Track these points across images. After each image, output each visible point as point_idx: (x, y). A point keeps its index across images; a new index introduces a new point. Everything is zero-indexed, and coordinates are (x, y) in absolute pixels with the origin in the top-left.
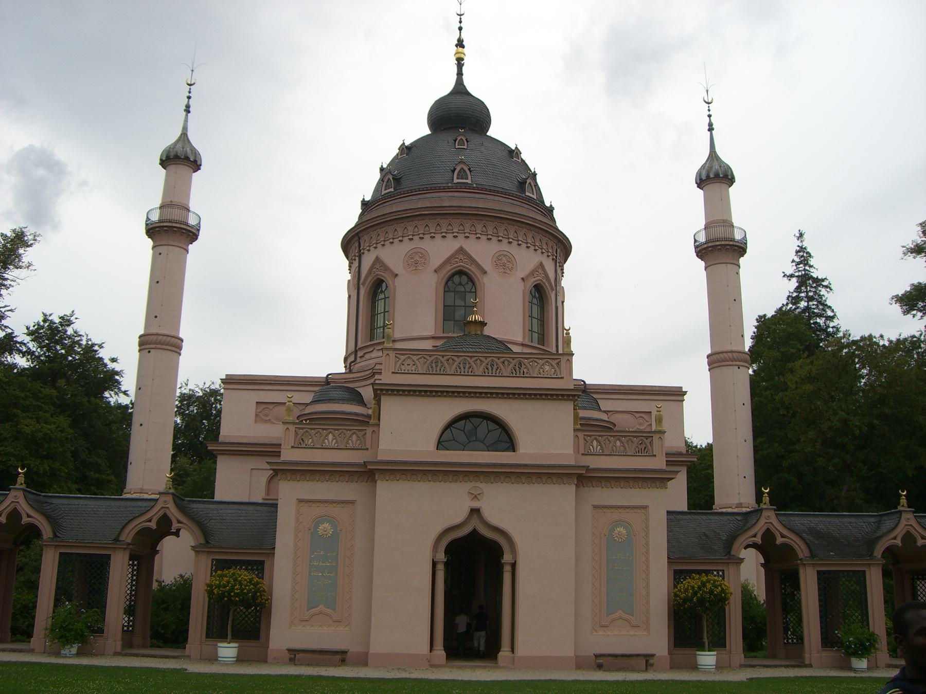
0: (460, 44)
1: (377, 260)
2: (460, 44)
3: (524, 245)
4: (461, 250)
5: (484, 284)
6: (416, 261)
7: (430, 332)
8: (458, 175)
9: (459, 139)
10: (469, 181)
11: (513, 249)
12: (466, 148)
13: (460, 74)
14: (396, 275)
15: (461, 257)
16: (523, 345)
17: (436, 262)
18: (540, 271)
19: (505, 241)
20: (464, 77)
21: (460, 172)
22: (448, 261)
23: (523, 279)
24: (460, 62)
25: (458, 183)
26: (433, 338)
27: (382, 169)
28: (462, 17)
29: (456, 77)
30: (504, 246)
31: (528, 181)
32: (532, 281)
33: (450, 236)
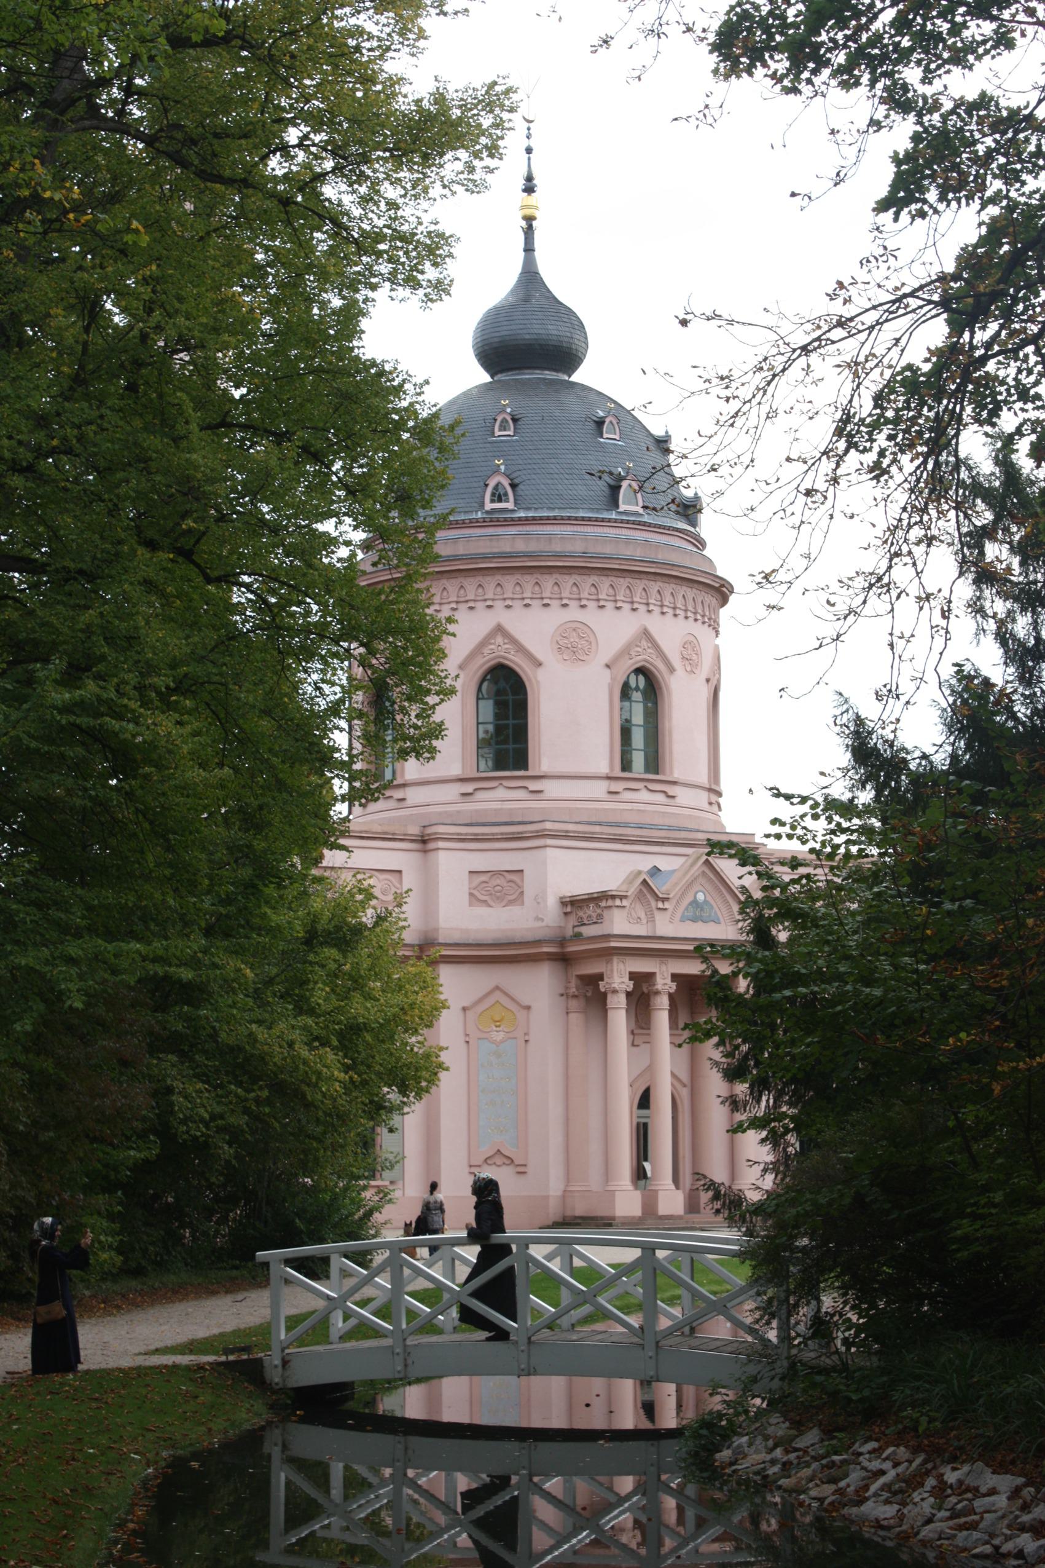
0: (529, 189)
2: (529, 189)
3: (610, 605)
4: (499, 629)
5: (538, 682)
8: (493, 495)
9: (499, 419)
11: (591, 617)
12: (511, 433)
13: (529, 249)
15: (499, 640)
16: (609, 778)
18: (644, 643)
19: (573, 604)
20: (537, 254)
21: (496, 487)
24: (529, 232)
25: (493, 511)
28: (531, 125)
29: (521, 255)
30: (573, 613)
31: (625, 484)
33: (480, 605)
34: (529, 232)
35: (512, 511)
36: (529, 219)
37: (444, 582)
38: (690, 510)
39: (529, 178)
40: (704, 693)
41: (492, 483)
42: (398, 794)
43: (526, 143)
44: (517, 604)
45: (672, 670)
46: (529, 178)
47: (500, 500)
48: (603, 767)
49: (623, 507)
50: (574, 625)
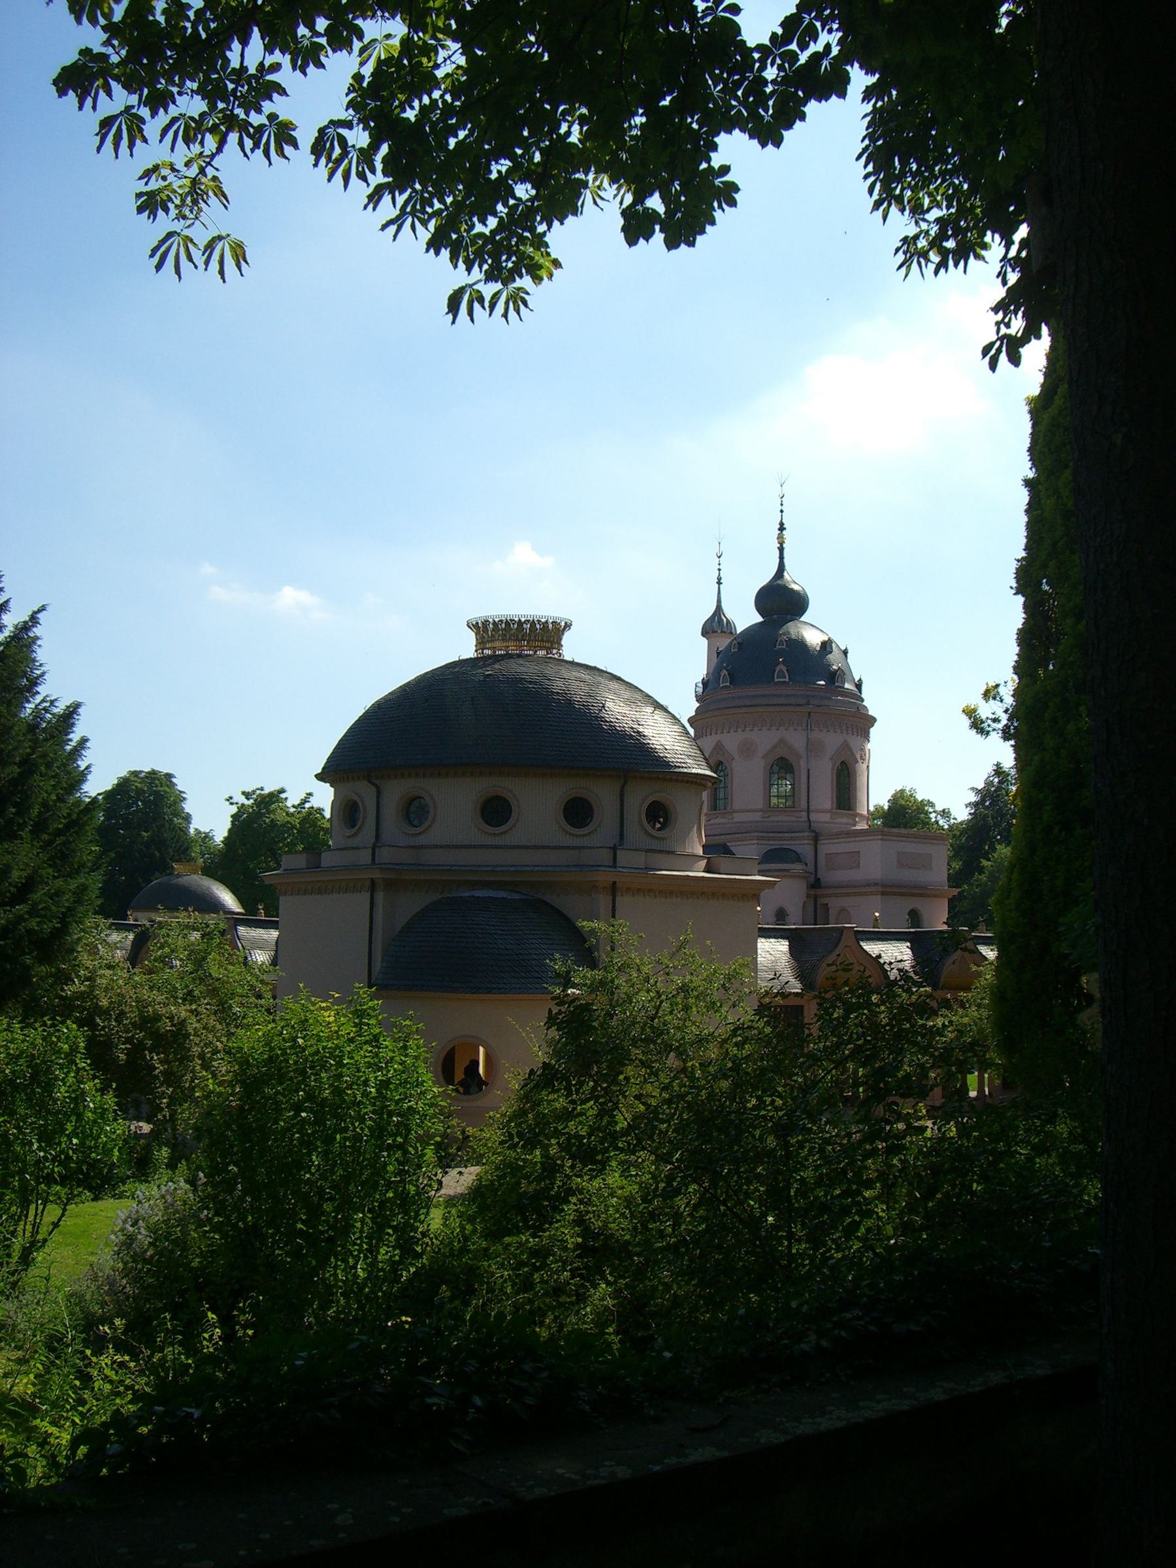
0: (782, 528)
1: (719, 747)
2: (782, 528)
6: (747, 750)
10: (787, 680)
13: (781, 557)
16: (830, 811)
24: (781, 549)
29: (778, 560)
34: (781, 549)
39: (782, 524)
41: (777, 669)
43: (780, 508)
46: (782, 524)
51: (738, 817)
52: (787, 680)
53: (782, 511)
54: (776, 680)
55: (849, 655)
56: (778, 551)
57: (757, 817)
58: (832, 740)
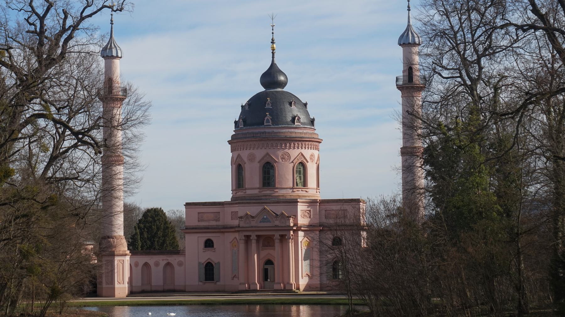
0: (273, 42)
1: (239, 156)
2: (273, 42)
7: (258, 186)
10: (270, 124)
13: (273, 57)
14: (245, 163)
15: (268, 156)
17: (258, 158)
21: (267, 120)
22: (263, 158)
23: (292, 162)
24: (273, 53)
26: (259, 188)
27: (242, 106)
32: (297, 162)
34: (273, 53)
35: (271, 125)
36: (273, 50)
37: (255, 143)
38: (312, 122)
40: (315, 166)
41: (266, 118)
42: (244, 191)
44: (272, 148)
45: (308, 162)
47: (268, 123)
48: (291, 186)
49: (296, 124)
50: (285, 153)
51: (249, 192)
52: (270, 124)
53: (273, 33)
54: (265, 124)
55: (308, 106)
56: (271, 54)
57: (256, 192)
58: (294, 153)
